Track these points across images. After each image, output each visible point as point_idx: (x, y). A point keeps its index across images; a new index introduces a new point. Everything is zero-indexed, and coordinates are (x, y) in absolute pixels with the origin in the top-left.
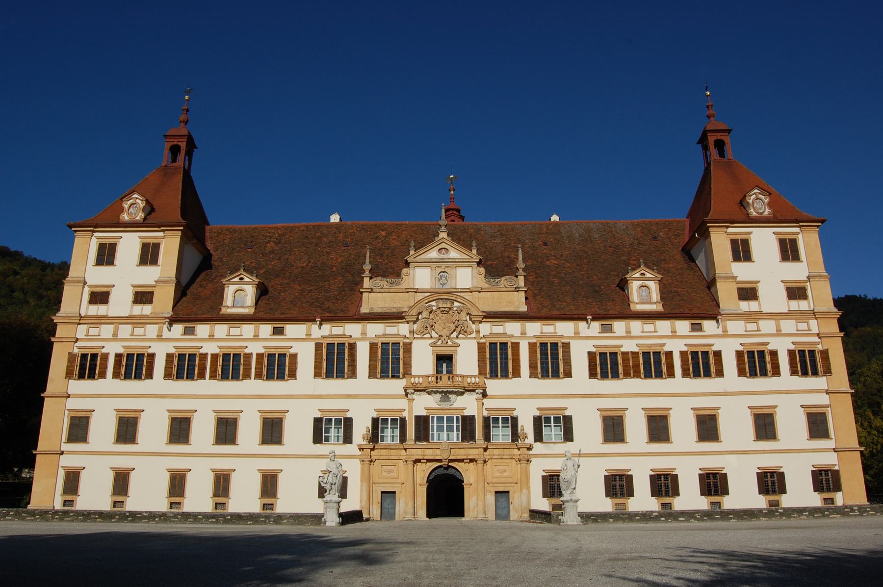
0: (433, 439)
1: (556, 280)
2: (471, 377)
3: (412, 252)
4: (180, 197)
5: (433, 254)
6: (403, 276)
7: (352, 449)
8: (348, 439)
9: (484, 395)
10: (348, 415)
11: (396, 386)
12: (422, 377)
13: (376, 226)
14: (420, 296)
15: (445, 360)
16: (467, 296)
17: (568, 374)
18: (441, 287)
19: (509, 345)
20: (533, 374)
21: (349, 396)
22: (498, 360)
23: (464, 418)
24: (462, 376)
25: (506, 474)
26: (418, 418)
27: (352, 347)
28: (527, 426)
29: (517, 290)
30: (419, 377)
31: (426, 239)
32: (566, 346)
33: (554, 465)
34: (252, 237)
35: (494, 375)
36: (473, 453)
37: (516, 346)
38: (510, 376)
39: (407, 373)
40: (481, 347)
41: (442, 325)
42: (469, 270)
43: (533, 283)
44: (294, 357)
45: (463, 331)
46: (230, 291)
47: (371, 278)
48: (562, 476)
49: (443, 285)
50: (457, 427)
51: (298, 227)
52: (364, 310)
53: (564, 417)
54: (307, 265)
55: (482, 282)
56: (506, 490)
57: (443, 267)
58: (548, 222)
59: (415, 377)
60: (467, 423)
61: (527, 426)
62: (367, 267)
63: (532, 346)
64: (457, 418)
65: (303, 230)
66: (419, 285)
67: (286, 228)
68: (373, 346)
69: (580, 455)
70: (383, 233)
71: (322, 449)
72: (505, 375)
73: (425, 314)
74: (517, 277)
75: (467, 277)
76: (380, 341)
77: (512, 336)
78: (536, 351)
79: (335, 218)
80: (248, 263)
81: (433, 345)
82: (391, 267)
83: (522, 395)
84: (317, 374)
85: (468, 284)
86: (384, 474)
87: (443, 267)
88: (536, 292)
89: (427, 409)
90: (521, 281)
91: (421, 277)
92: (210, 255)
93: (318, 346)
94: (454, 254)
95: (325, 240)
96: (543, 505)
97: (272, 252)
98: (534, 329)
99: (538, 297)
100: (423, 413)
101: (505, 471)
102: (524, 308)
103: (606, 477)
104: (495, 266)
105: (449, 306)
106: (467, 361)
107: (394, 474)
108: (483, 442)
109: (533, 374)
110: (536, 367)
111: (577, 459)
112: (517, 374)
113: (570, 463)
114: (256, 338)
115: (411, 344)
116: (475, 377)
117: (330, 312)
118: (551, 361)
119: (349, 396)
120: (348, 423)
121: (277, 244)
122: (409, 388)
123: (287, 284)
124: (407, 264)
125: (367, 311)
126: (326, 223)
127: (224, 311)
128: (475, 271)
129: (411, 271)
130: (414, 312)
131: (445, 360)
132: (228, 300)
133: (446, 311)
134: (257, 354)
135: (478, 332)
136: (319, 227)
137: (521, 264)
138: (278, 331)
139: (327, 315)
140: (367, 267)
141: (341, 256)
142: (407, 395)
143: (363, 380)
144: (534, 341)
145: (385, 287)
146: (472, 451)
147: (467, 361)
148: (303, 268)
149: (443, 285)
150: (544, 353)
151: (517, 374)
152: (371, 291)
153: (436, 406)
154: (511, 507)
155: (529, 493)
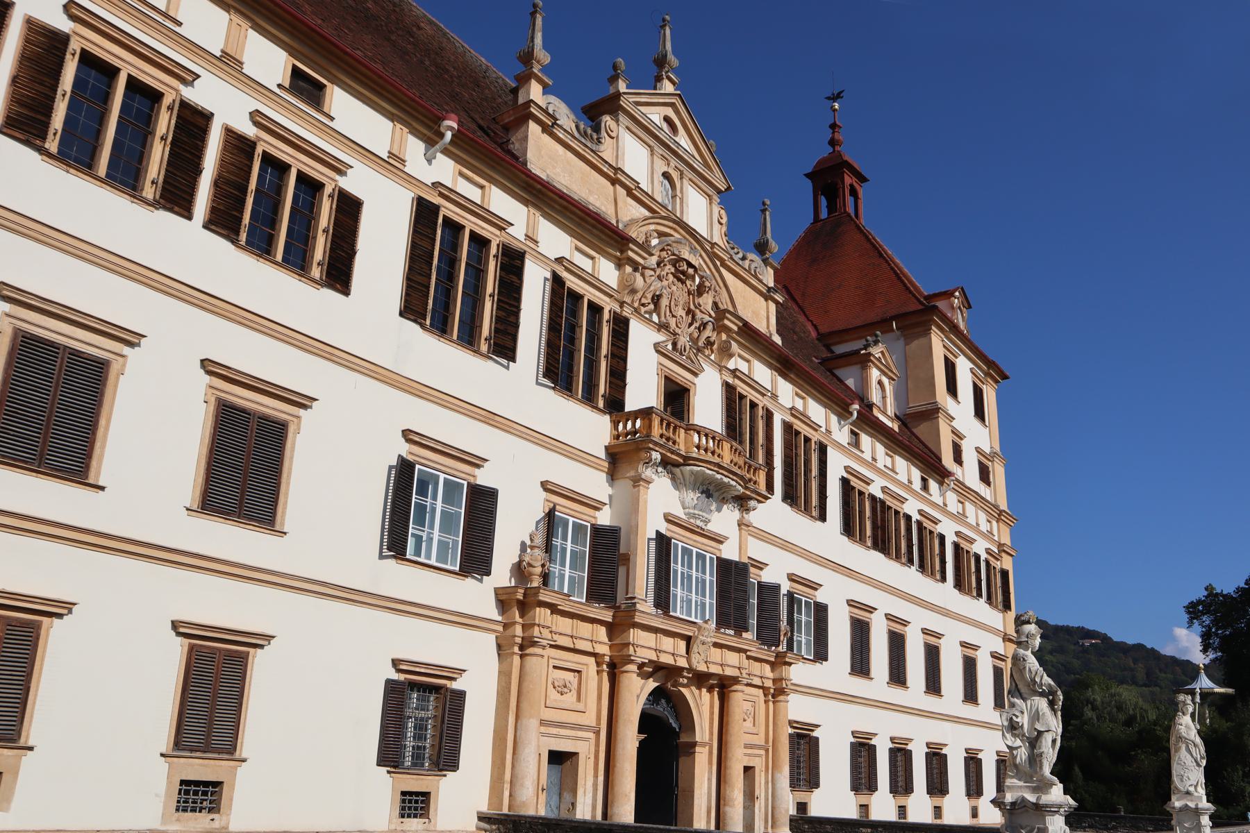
7: (477, 596)
8: (476, 560)
10: (484, 478)
11: (592, 429)
21: (490, 418)
36: (730, 663)
44: (349, 207)
71: (399, 579)
84: (412, 309)
86: (553, 694)
93: (424, 214)
107: (570, 699)
119: (490, 418)
120: (482, 503)
138: (306, 88)
143: (518, 385)
146: (733, 658)
153: (679, 512)
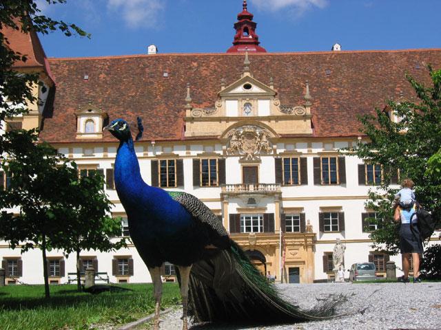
0: (243, 231)
1: (336, 106)
2: (271, 185)
3: (223, 88)
4: (30, 40)
5: (240, 89)
6: (216, 107)
9: (281, 199)
12: (234, 185)
13: (188, 57)
14: (231, 123)
15: (250, 174)
16: (266, 123)
17: (343, 181)
18: (246, 115)
19: (299, 159)
20: (317, 182)
22: (290, 172)
23: (266, 215)
24: (265, 185)
26: (232, 216)
27: (180, 164)
28: (313, 221)
29: (305, 117)
30: (231, 185)
31: (232, 77)
32: (342, 161)
33: (330, 248)
34: (86, 68)
35: (287, 184)
37: (304, 161)
38: (300, 183)
39: (222, 181)
40: (278, 162)
41: (247, 147)
42: (268, 102)
43: (317, 109)
45: (264, 152)
46: (82, 121)
47: (191, 109)
48: (334, 255)
49: (248, 113)
51: (124, 59)
52: (188, 134)
53: (340, 213)
54: (136, 95)
55: (279, 113)
56: (297, 266)
57: (248, 99)
58: (332, 52)
59: (228, 185)
60: (269, 218)
61: (313, 221)
62: (188, 99)
63: (316, 161)
65: (128, 62)
66: (229, 114)
67: (114, 60)
68: (196, 163)
69: (346, 242)
70: (195, 64)
72: (296, 183)
73: (234, 138)
74: (305, 107)
75: (264, 108)
76: (201, 159)
77: (301, 153)
79: (152, 50)
80: (87, 93)
81: (241, 161)
82: (208, 99)
83: (309, 199)
85: (267, 114)
87: (248, 99)
88: (320, 117)
89: (238, 209)
90: (308, 111)
91: (231, 108)
92: (54, 84)
94: (255, 89)
95: (147, 70)
96: (325, 276)
97: (105, 82)
98: (317, 150)
99: (321, 122)
100: (236, 212)
102: (310, 131)
104: (288, 97)
105: (252, 131)
106: (267, 171)
109: (317, 182)
111: (344, 244)
112: (304, 182)
113: (339, 246)
114: (105, 158)
115: (225, 160)
116: (274, 185)
117: (161, 136)
118: (331, 173)
121: (107, 74)
122: (225, 194)
123: (123, 111)
124: (220, 97)
125: (190, 136)
126: (146, 56)
127: (78, 137)
128: (273, 102)
129: (223, 103)
130: (226, 137)
131: (250, 174)
132: (81, 129)
133: (251, 136)
134: (108, 170)
135: (275, 151)
136: (141, 58)
137: (307, 96)
139: (160, 139)
140: (188, 99)
141: (163, 86)
142: (222, 199)
144: (317, 156)
145: (203, 116)
147: (267, 171)
148: (132, 96)
149: (248, 113)
151: (304, 182)
152: (192, 120)
155: (313, 268)
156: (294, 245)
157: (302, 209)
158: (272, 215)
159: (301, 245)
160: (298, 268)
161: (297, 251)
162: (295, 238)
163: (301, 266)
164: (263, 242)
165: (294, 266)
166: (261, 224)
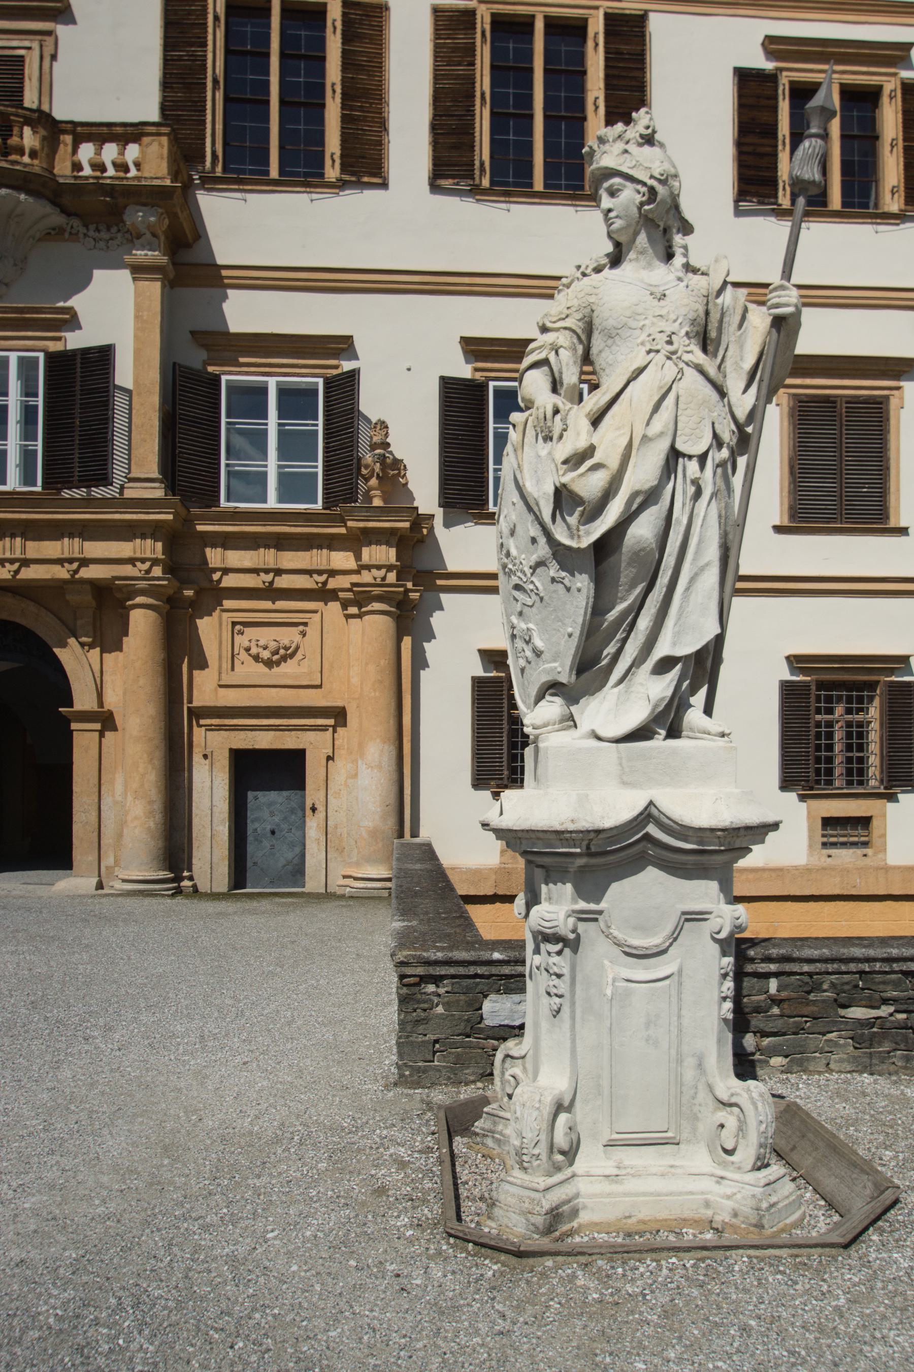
20: (450, 167)
23: (60, 363)
25: (288, 670)
35: (244, 168)
38: (332, 172)
50: (29, 413)
56: (289, 741)
64: (27, 367)
72: (303, 170)
78: (470, 50)
101: (285, 655)
103: (788, 691)
108: (157, 492)
110: (467, 130)
112: (365, 164)
150: (511, 73)
151: (365, 164)
154: (313, 827)
156: (271, 593)
157: (342, 346)
158: (101, 358)
159: (324, 594)
160: (299, 756)
161: (288, 636)
162: (281, 543)
163: (314, 743)
164: (46, 560)
165: (264, 741)
166: (28, 433)
